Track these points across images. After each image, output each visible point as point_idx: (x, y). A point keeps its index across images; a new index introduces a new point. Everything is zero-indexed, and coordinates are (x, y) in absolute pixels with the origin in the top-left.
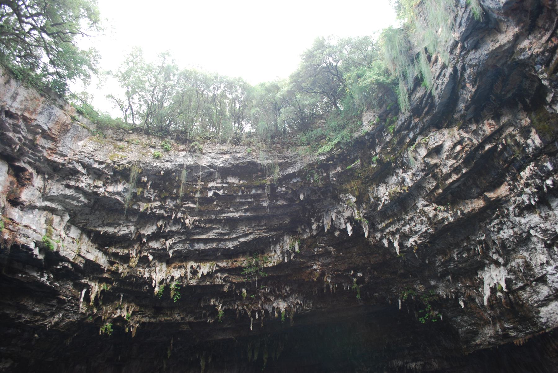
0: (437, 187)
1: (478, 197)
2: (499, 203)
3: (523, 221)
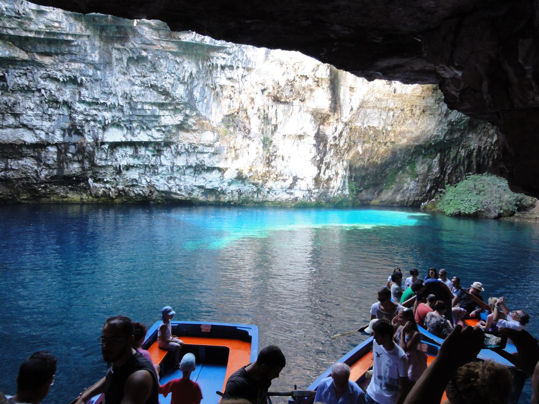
0: (12, 29)
1: (27, 52)
2: (41, 65)
3: (42, 82)
